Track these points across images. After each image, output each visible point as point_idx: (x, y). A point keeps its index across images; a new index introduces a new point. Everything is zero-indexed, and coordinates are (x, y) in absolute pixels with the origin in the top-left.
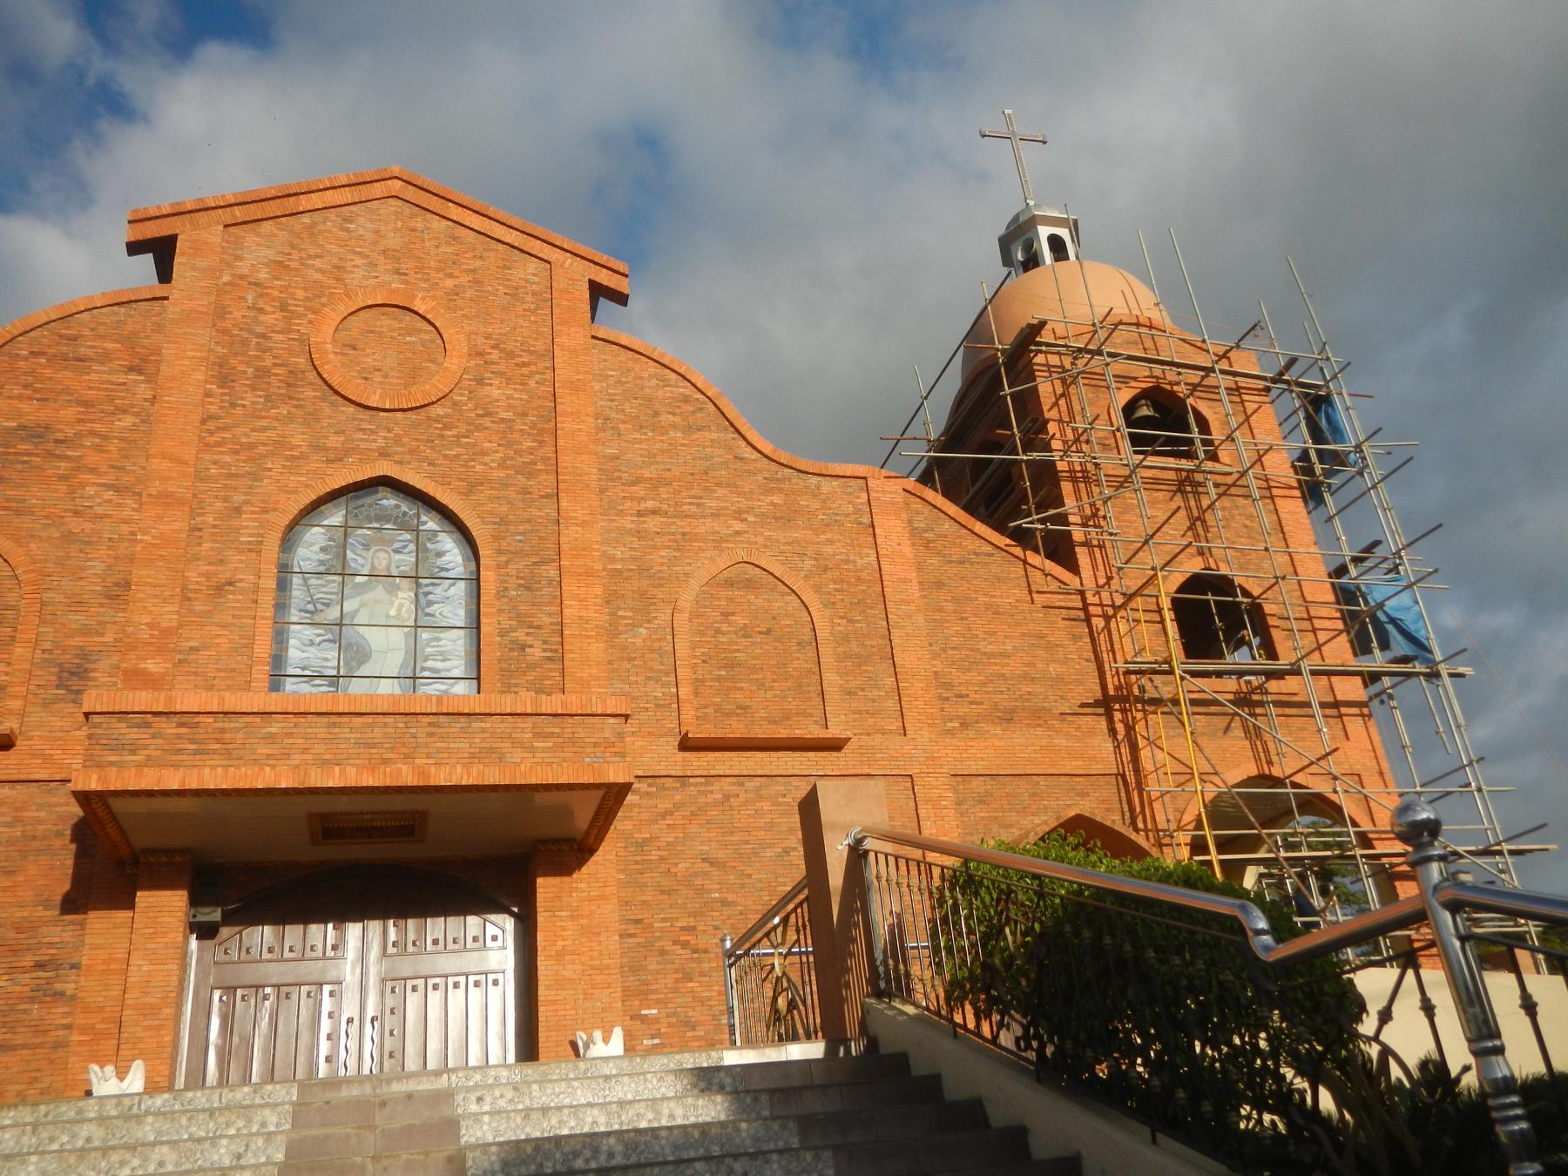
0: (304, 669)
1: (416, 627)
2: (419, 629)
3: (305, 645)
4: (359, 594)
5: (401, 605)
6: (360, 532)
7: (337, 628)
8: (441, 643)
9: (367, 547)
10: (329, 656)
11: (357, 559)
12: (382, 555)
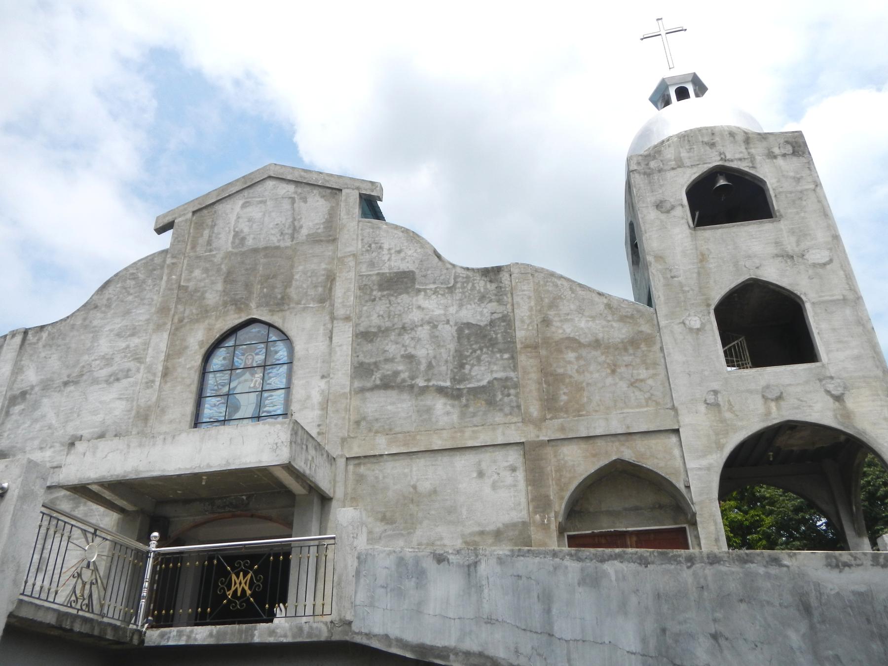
0: (210, 418)
1: (262, 391)
2: (263, 392)
3: (212, 407)
4: (238, 378)
5: (256, 381)
6: (241, 347)
7: (226, 396)
8: (273, 397)
9: (243, 354)
10: (222, 411)
11: (239, 362)
12: (250, 357)
